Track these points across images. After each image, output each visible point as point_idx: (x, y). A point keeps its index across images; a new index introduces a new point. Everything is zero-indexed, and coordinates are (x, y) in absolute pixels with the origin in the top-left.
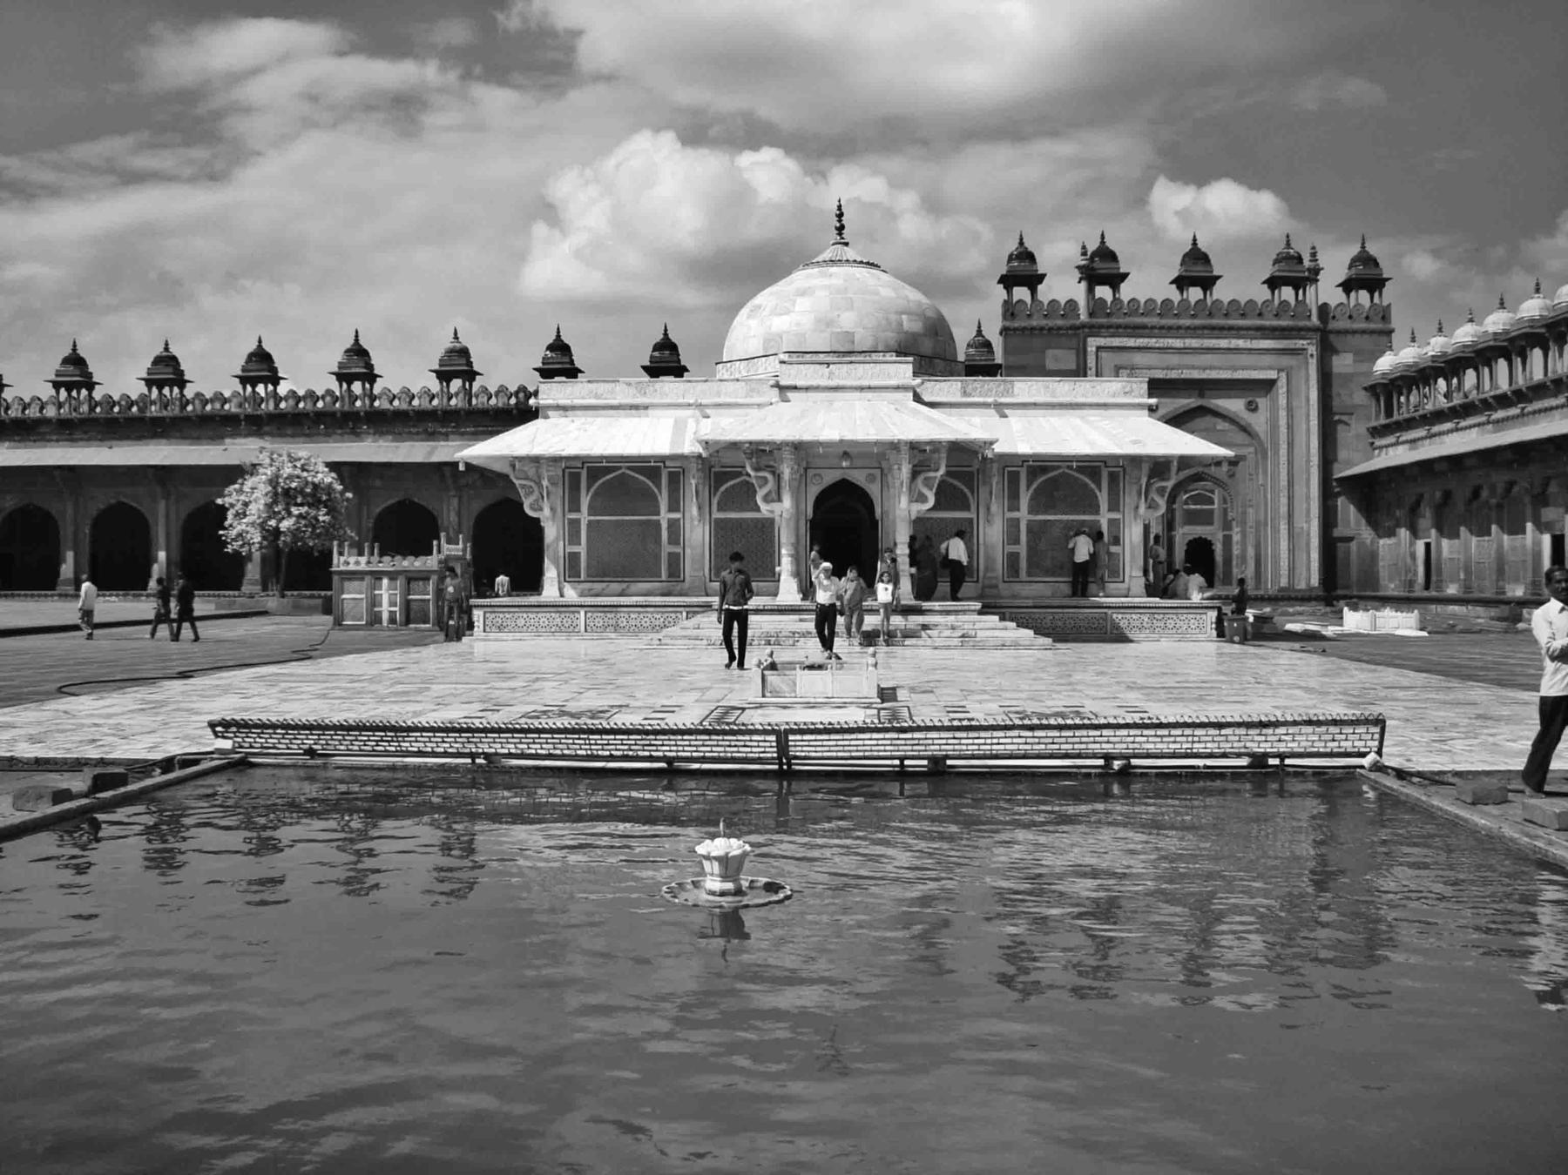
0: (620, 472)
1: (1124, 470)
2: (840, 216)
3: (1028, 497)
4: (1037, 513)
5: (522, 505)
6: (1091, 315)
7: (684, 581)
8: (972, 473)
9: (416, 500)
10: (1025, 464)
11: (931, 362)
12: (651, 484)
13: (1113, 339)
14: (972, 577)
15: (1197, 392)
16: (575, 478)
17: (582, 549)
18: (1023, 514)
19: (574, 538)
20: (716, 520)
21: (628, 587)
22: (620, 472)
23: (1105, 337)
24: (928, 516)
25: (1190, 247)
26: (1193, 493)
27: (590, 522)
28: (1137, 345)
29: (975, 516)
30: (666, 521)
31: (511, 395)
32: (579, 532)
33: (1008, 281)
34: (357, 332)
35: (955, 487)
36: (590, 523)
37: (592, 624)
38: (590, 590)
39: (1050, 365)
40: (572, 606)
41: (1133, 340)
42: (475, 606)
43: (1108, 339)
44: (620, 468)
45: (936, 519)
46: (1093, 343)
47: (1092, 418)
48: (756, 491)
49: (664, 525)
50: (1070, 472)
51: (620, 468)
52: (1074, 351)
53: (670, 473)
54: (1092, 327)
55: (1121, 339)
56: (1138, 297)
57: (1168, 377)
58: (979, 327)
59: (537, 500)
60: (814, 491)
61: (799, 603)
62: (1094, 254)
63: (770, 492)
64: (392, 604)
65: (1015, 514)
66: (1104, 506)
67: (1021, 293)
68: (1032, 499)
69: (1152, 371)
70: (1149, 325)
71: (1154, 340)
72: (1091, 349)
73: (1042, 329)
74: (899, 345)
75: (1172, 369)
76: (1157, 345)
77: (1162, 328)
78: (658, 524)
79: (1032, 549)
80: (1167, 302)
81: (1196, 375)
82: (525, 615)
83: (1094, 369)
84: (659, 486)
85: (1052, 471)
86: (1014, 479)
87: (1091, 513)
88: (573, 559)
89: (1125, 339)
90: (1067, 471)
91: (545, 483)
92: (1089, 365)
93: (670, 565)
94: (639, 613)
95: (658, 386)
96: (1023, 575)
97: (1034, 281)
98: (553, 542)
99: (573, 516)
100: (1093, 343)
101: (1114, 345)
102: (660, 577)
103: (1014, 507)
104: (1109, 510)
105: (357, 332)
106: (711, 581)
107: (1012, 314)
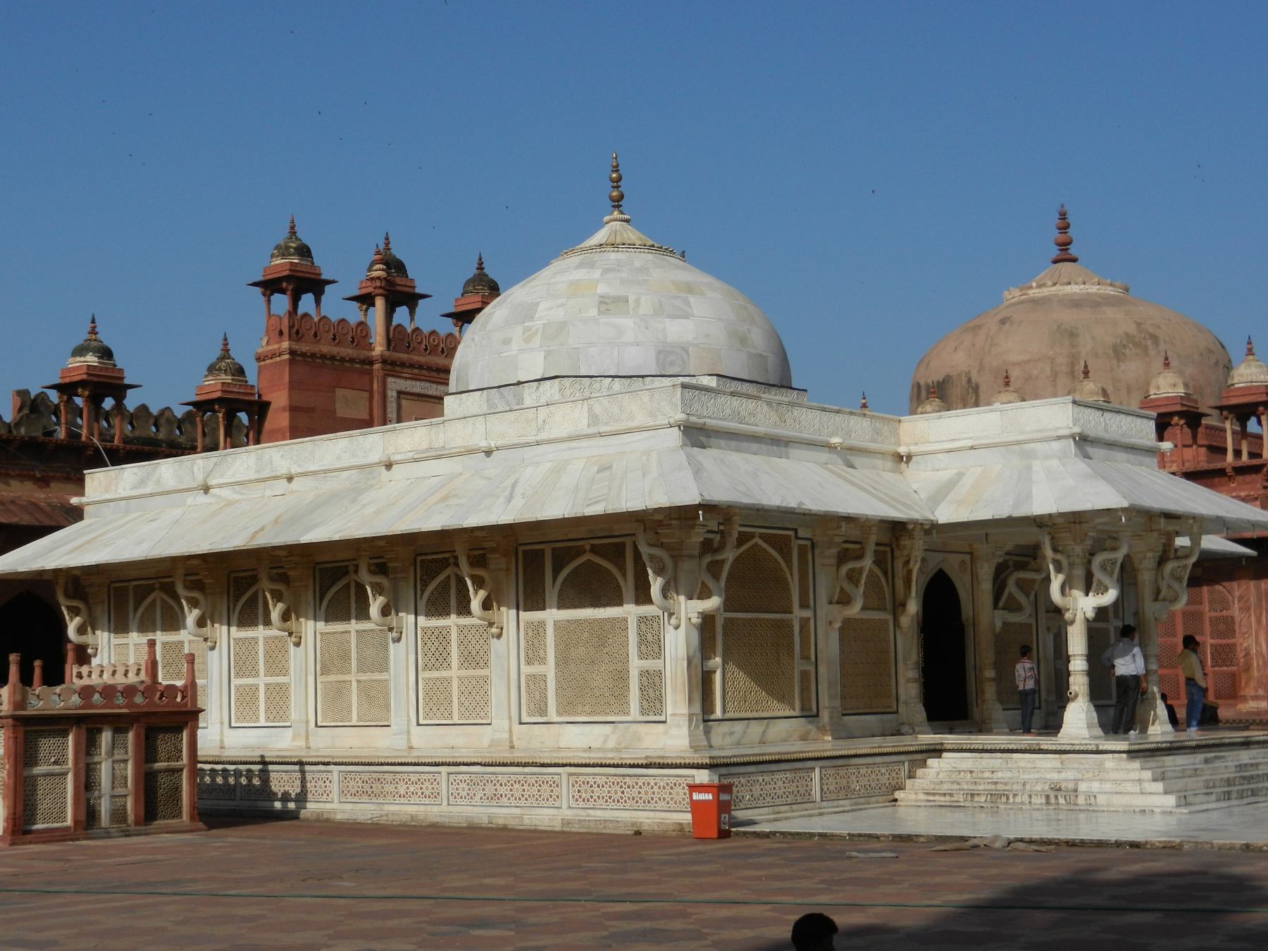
2: (620, 179)
7: (817, 715)
13: (413, 383)
21: (768, 723)
23: (406, 378)
25: (475, 271)
39: (342, 411)
41: (434, 386)
43: (409, 382)
44: (752, 536)
46: (394, 384)
52: (366, 395)
54: (393, 363)
55: (423, 384)
61: (1170, 738)
72: (392, 394)
73: (333, 358)
78: (788, 625)
82: (761, 779)
89: (427, 384)
92: (389, 415)
94: (868, 765)
107: (297, 332)
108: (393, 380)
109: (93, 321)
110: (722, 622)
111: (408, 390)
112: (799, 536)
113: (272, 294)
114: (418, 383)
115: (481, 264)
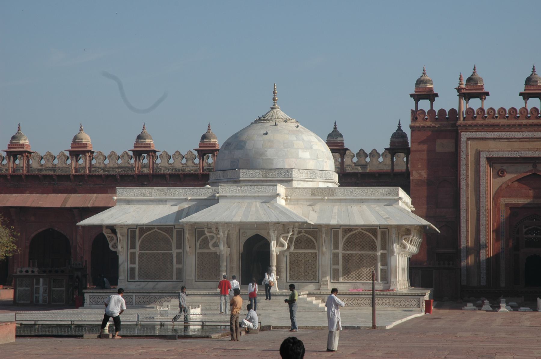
0: (154, 230)
1: (388, 230)
3: (343, 243)
4: (347, 250)
5: (109, 245)
6: (464, 118)
7: (183, 281)
8: (317, 231)
9: (56, 229)
10: (341, 227)
11: (313, 172)
12: (168, 237)
14: (316, 280)
15: (532, 164)
16: (133, 233)
17: (136, 266)
18: (340, 251)
19: (133, 261)
20: (198, 253)
22: (154, 230)
23: (472, 132)
24: (293, 251)
26: (530, 228)
27: (140, 253)
28: (493, 137)
29: (317, 252)
30: (175, 253)
31: (119, 157)
32: (135, 258)
33: (417, 97)
34: (19, 125)
35: (309, 238)
36: (140, 255)
37: (138, 301)
38: (139, 285)
40: (129, 293)
42: (85, 293)
43: (475, 133)
44: (154, 228)
45: (299, 253)
47: (372, 206)
48: (209, 242)
49: (174, 255)
50: (363, 231)
51: (154, 228)
53: (177, 230)
54: (465, 126)
55: (483, 133)
56: (494, 107)
57: (511, 156)
58: (399, 124)
59: (115, 243)
60: (243, 240)
62: (469, 80)
63: (215, 243)
64: (45, 291)
65: (336, 251)
66: (379, 246)
67: (424, 105)
68: (344, 244)
69: (502, 152)
70: (500, 124)
71: (503, 133)
74: (296, 165)
75: (514, 152)
76: (505, 136)
77: (509, 125)
78: (171, 255)
79: (344, 267)
80: (513, 110)
81: (530, 154)
83: (465, 152)
84: (171, 236)
85: (353, 231)
86: (336, 234)
87: (372, 250)
88: (132, 270)
89: (485, 133)
90: (361, 231)
91: (119, 235)
92: (462, 149)
93: (177, 274)
94: (160, 296)
95: (171, 190)
96: (341, 280)
97: (431, 96)
98: (122, 263)
99: (132, 251)
100: (464, 136)
101: (477, 137)
102: (172, 279)
103: (336, 247)
104: (381, 249)
105: (19, 125)
106: (195, 281)
108: (465, 133)
109: (335, 123)
110: (138, 254)
111: (473, 137)
112: (175, 227)
113: (419, 100)
114: (480, 133)
115: (534, 69)
